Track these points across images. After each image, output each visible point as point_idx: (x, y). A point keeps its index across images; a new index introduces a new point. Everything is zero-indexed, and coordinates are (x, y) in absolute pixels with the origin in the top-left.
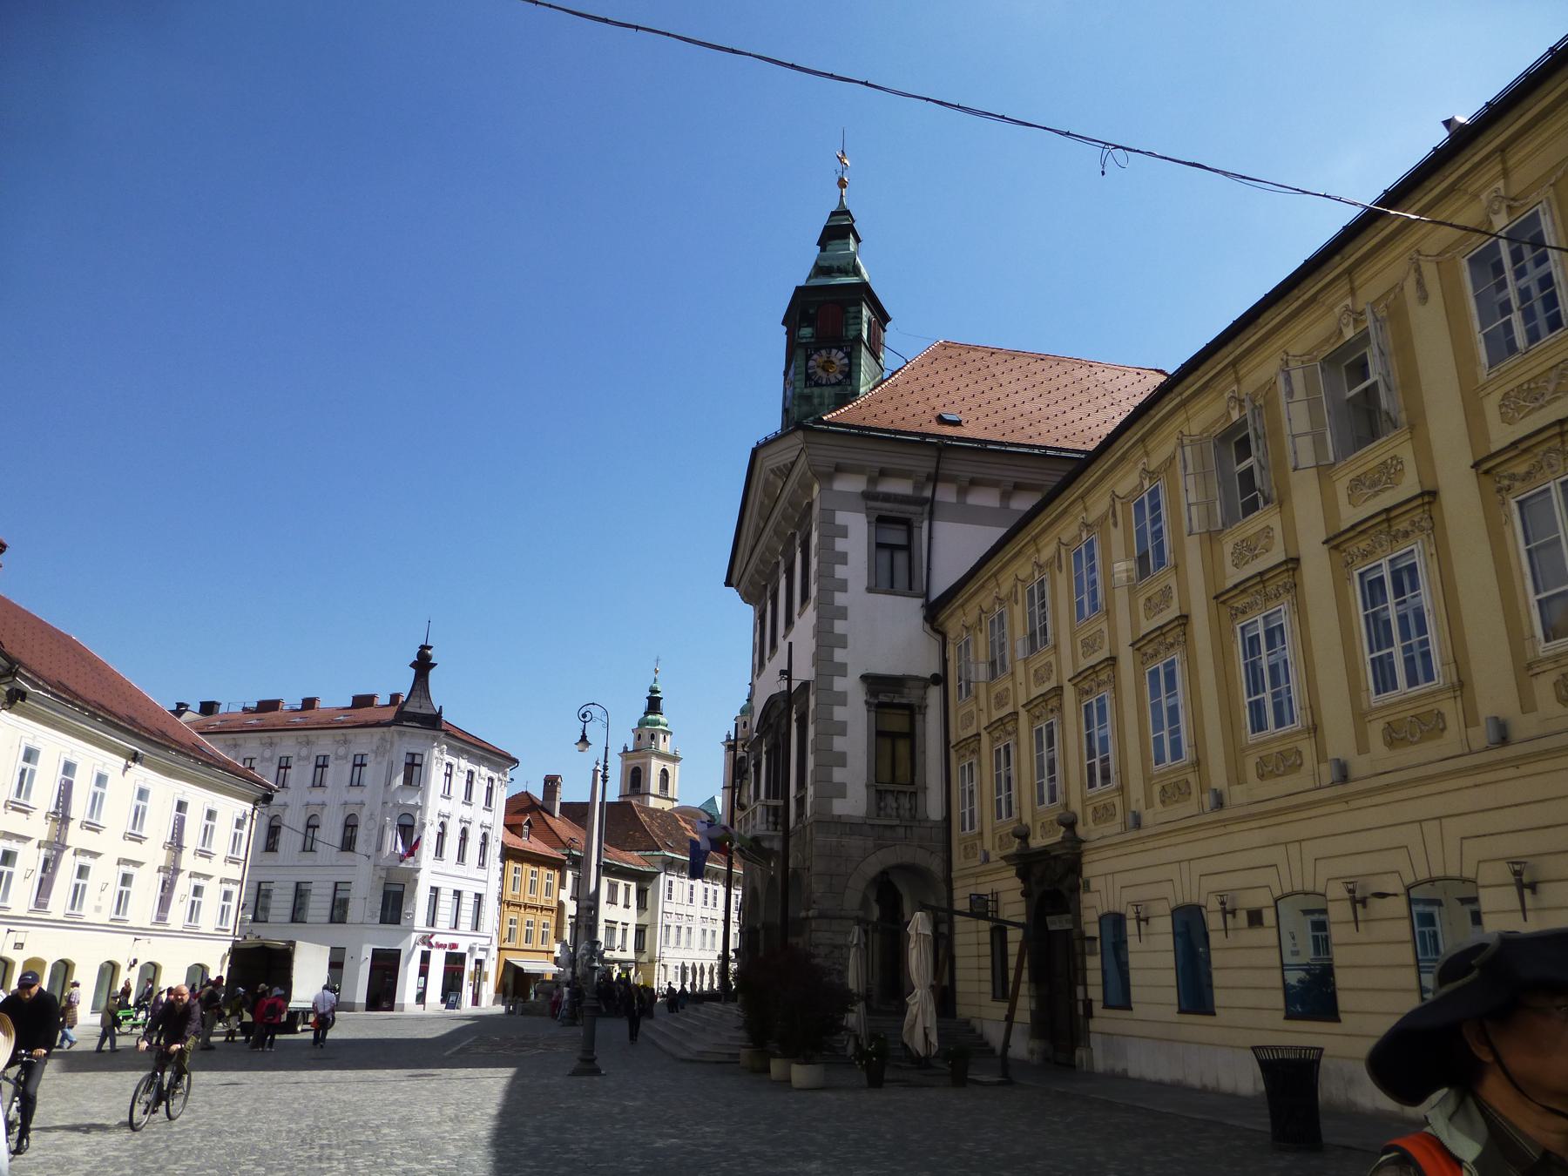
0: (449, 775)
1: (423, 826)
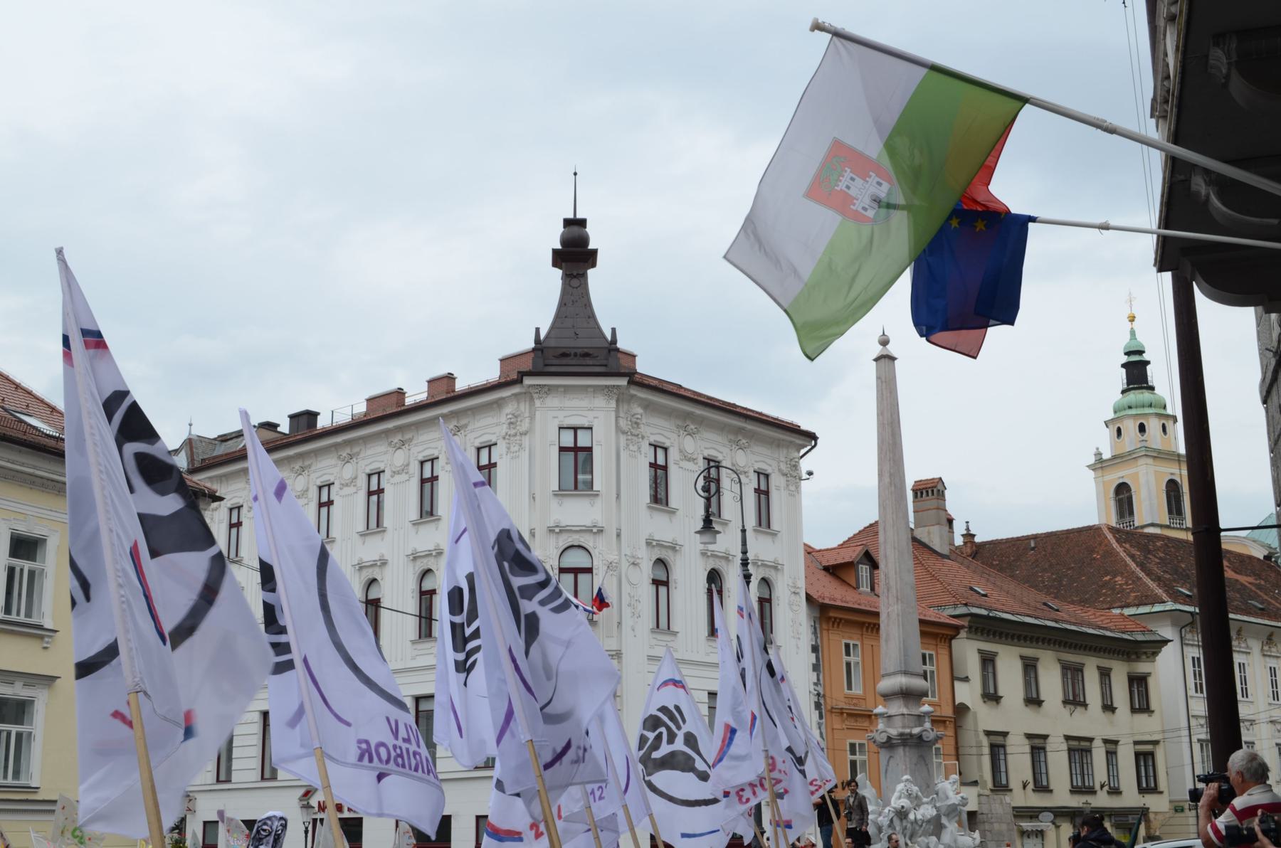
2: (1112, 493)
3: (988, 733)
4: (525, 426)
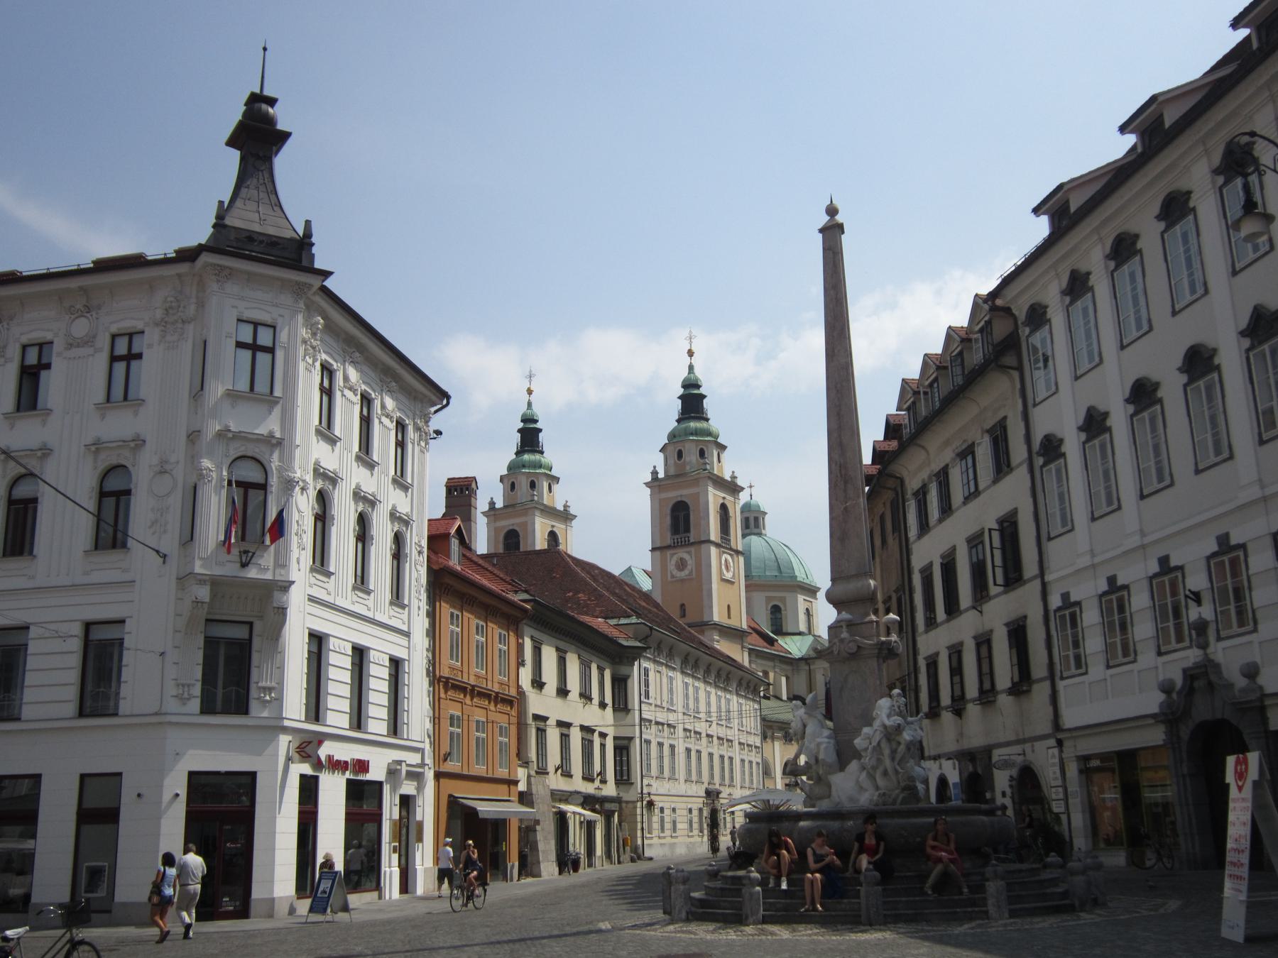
0: (327, 392)
1: (289, 485)
2: (501, 538)
3: (537, 717)
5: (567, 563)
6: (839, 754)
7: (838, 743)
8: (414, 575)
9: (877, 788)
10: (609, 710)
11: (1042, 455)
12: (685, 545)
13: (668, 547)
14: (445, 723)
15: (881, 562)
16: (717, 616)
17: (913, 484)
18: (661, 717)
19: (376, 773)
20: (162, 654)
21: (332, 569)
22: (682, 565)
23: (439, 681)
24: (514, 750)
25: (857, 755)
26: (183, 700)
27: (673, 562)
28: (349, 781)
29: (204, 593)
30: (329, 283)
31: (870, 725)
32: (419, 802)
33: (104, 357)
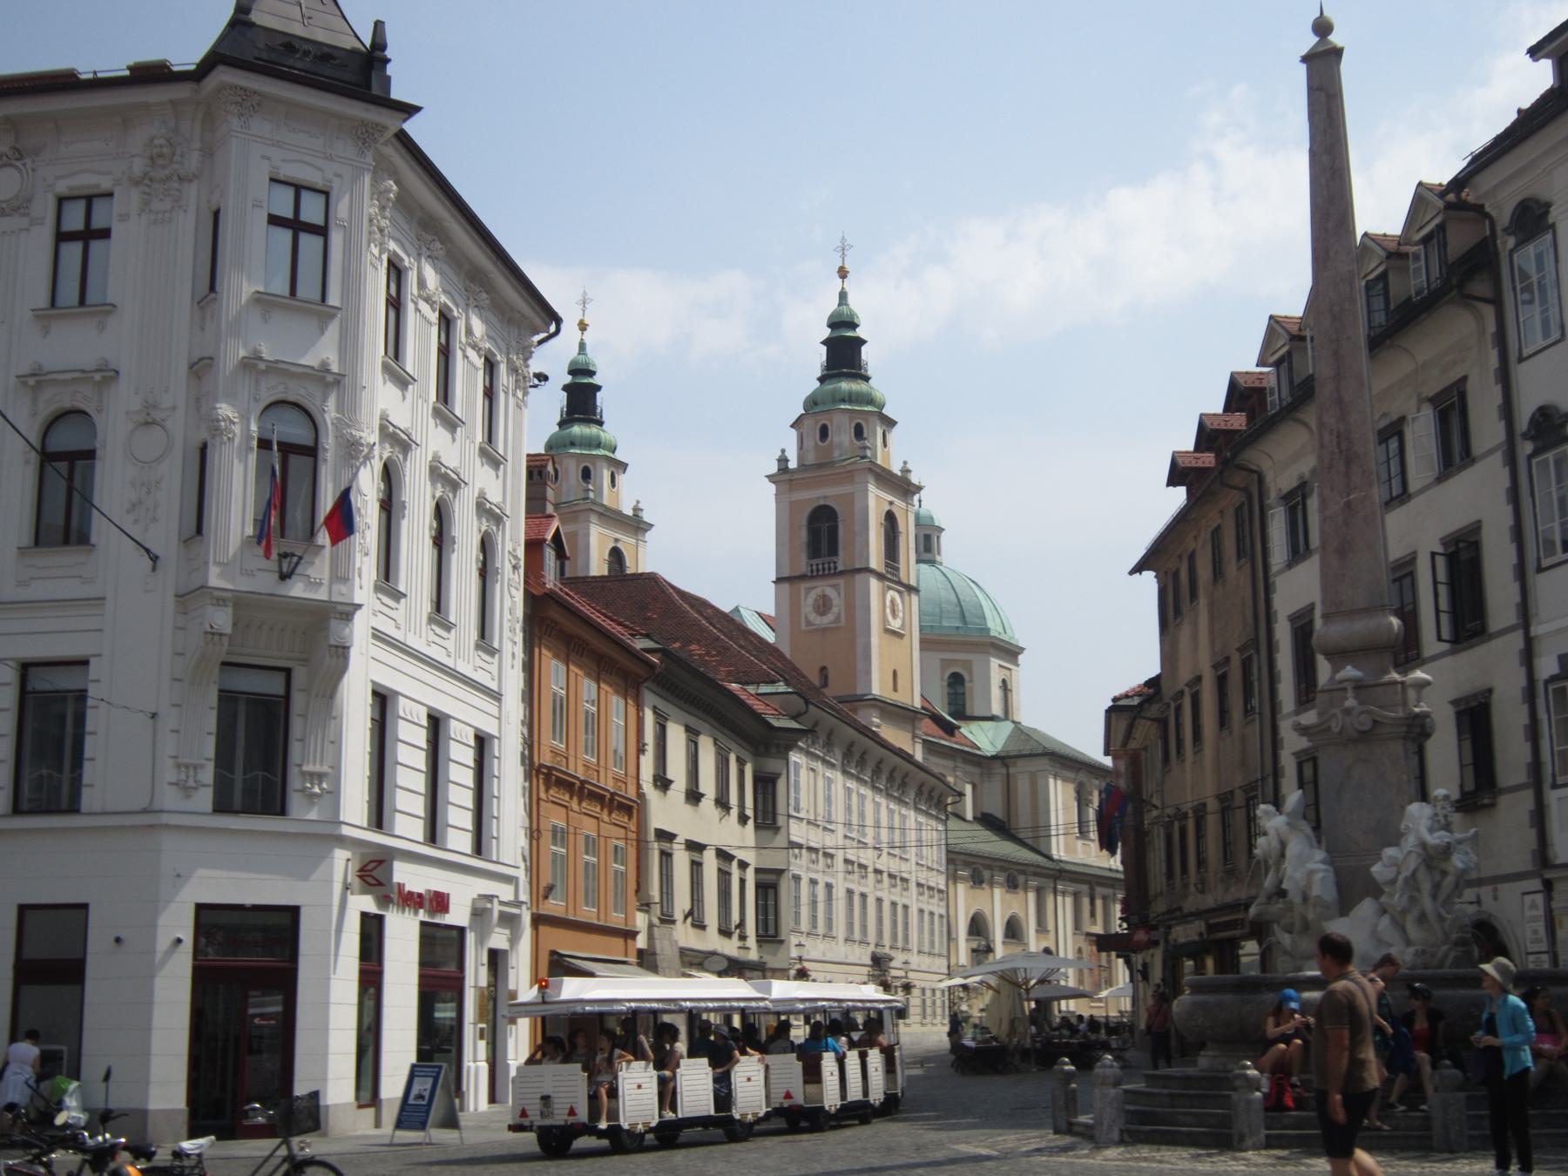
0: (395, 304)
1: (353, 451)
4: (193, 161)
5: (669, 597)
6: (1340, 887)
7: (1337, 873)
8: (508, 603)
9: (1408, 943)
10: (751, 823)
11: (1532, 438)
12: (830, 575)
13: (803, 577)
14: (546, 837)
15: (1211, 604)
16: (878, 686)
17: (1281, 481)
18: (815, 838)
19: (458, 915)
20: (154, 716)
21: (402, 588)
22: (823, 606)
23: (538, 772)
24: (632, 886)
25: (1374, 890)
26: (186, 790)
27: (810, 601)
28: (423, 924)
29: (222, 619)
30: (412, 127)
31: (1397, 844)
32: (512, 961)
33: (46, 234)
